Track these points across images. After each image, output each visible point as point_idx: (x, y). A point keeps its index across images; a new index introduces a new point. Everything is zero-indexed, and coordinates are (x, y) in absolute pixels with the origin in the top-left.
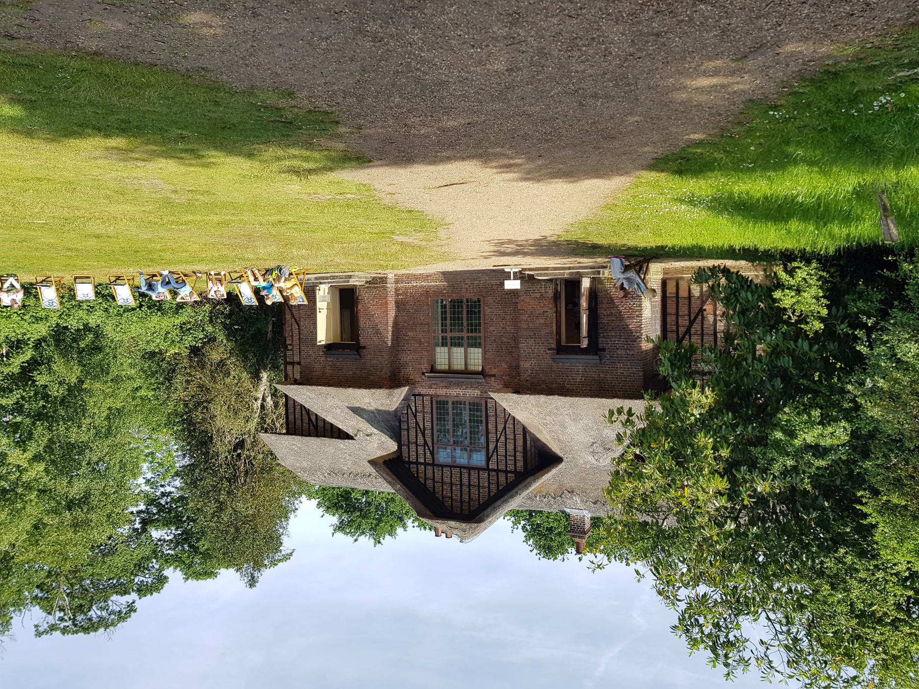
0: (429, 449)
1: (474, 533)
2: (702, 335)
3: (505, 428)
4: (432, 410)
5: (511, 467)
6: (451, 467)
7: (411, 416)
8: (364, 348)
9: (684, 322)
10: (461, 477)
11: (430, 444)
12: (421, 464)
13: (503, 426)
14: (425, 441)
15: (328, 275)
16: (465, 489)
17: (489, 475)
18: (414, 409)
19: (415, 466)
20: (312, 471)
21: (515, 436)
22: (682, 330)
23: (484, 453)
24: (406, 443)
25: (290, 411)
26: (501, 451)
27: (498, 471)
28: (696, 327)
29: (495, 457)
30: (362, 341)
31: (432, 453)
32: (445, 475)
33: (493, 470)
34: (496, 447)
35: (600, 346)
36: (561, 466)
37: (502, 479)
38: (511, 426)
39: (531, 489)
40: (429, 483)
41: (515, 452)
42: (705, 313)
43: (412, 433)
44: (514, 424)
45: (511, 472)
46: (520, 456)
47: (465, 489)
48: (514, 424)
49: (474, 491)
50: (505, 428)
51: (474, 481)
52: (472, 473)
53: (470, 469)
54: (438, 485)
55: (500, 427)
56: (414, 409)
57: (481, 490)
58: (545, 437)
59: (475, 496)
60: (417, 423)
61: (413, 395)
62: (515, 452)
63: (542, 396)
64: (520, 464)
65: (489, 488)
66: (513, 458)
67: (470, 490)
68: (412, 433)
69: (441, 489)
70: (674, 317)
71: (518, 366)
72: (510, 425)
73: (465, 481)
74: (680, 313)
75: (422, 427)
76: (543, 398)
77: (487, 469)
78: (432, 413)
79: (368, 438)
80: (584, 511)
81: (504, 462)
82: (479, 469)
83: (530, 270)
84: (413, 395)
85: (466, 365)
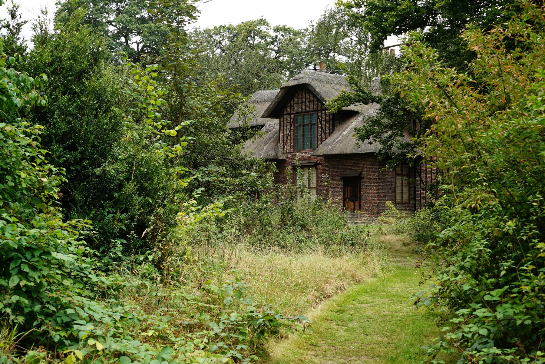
5: (285, 117)
11: (319, 123)
16: (304, 101)
26: (289, 125)
33: (292, 114)
34: (291, 127)
45: (285, 114)
47: (304, 101)
49: (300, 100)
55: (289, 137)
59: (300, 97)
72: (285, 139)
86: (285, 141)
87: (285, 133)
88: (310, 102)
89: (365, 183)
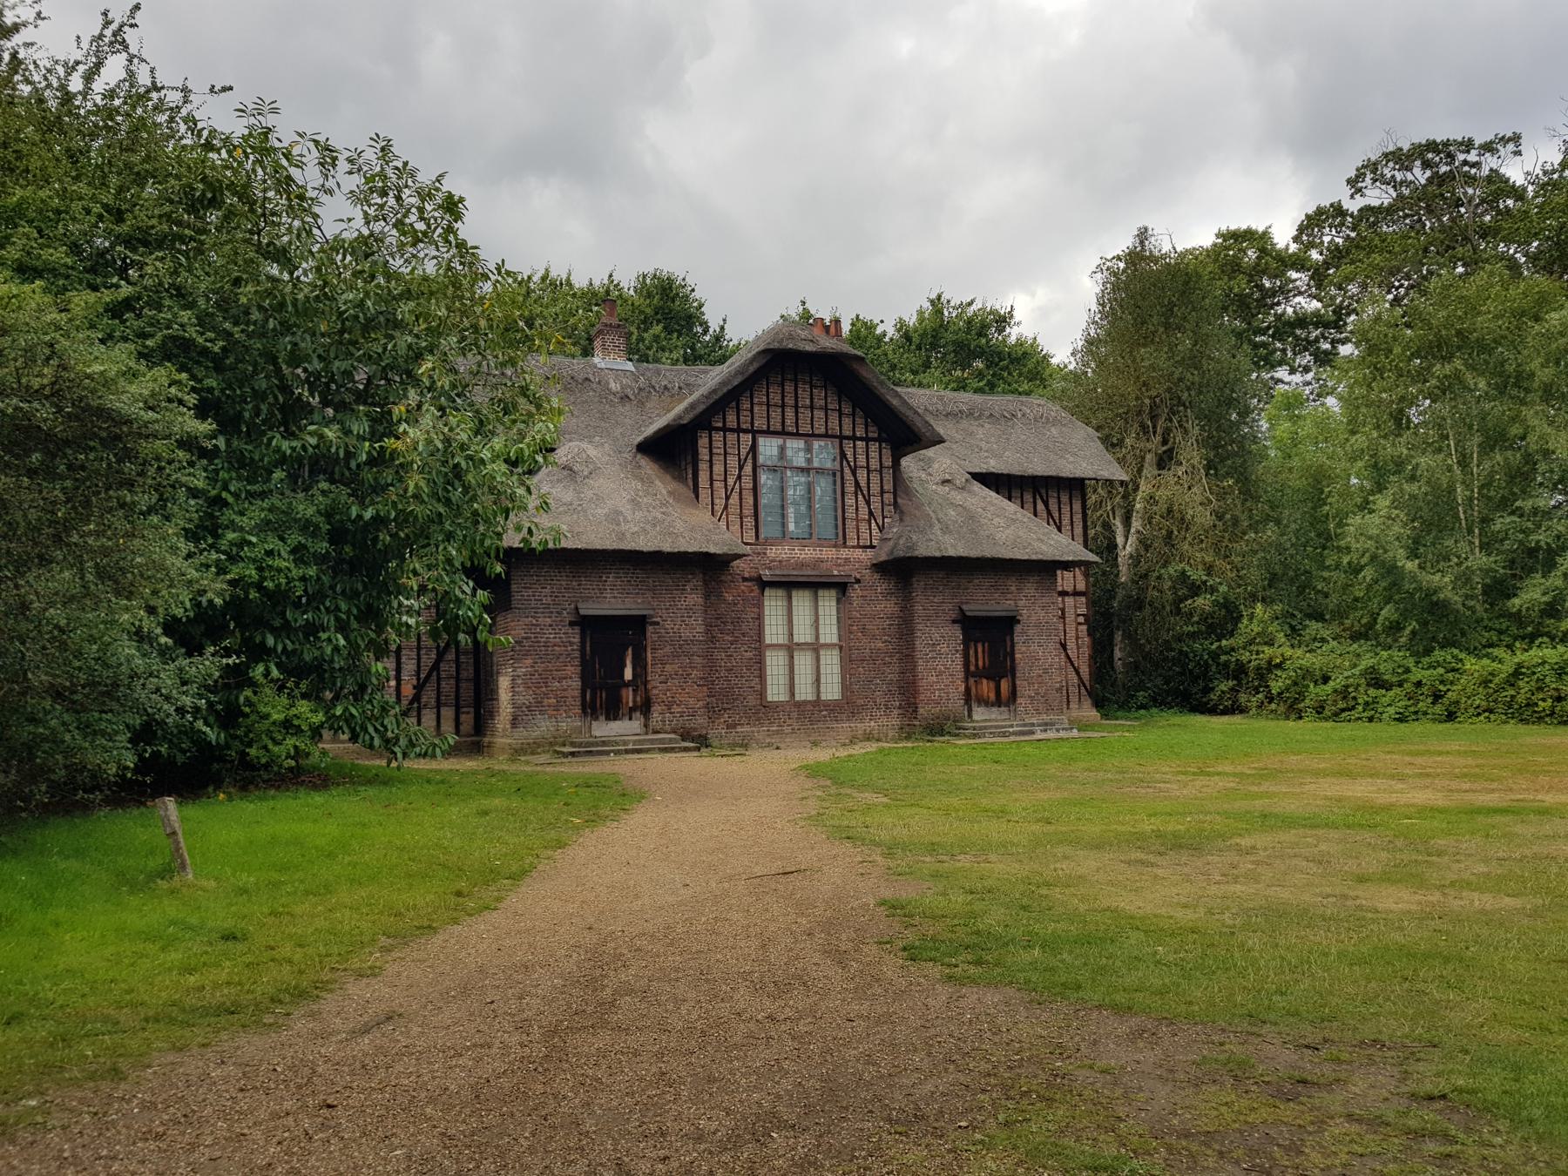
0: (848, 462)
1: (774, 332)
2: (419, 648)
3: (727, 498)
4: (844, 524)
5: (718, 437)
6: (813, 435)
7: (878, 514)
8: (954, 622)
9: (447, 668)
10: (797, 419)
11: (847, 470)
12: (861, 439)
13: (731, 501)
14: (854, 473)
15: (1012, 738)
16: (790, 401)
17: (752, 424)
18: (873, 524)
19: (870, 435)
20: (1042, 421)
21: (711, 484)
22: (451, 656)
23: (761, 460)
24: (885, 471)
25: (1080, 516)
26: (733, 462)
27: (739, 430)
28: (428, 660)
29: (743, 452)
30: (957, 633)
31: (843, 455)
32: (823, 422)
33: (746, 431)
34: (741, 468)
35: (577, 630)
36: (640, 439)
37: (731, 420)
38: (717, 501)
39: (685, 404)
40: (847, 410)
41: (711, 461)
42: (415, 682)
43: (875, 488)
44: (713, 504)
45: (718, 429)
46: (704, 453)
47: (790, 401)
48: (713, 504)
49: (776, 398)
50: (727, 498)
51: (776, 415)
52: (779, 428)
53: (783, 433)
54: (833, 405)
55: (734, 499)
56: (873, 524)
57: (765, 399)
58: (662, 485)
60: (868, 503)
61: (874, 547)
62: (711, 461)
63: (669, 550)
64: (703, 442)
65: (752, 404)
66: (715, 451)
67: (783, 399)
68: (875, 488)
69: (829, 400)
70: (464, 675)
71: (707, 597)
72: (720, 503)
73: (790, 413)
74: (453, 682)
75: (860, 497)
76: (667, 547)
77: (755, 433)
78: (844, 519)
79: (947, 477)
80: (603, 366)
81: (729, 444)
82: (768, 432)
83: (686, 749)
84: (874, 547)
85: (790, 598)
86: (719, 508)
87: (718, 485)
88: (812, 408)
89: (1023, 633)
